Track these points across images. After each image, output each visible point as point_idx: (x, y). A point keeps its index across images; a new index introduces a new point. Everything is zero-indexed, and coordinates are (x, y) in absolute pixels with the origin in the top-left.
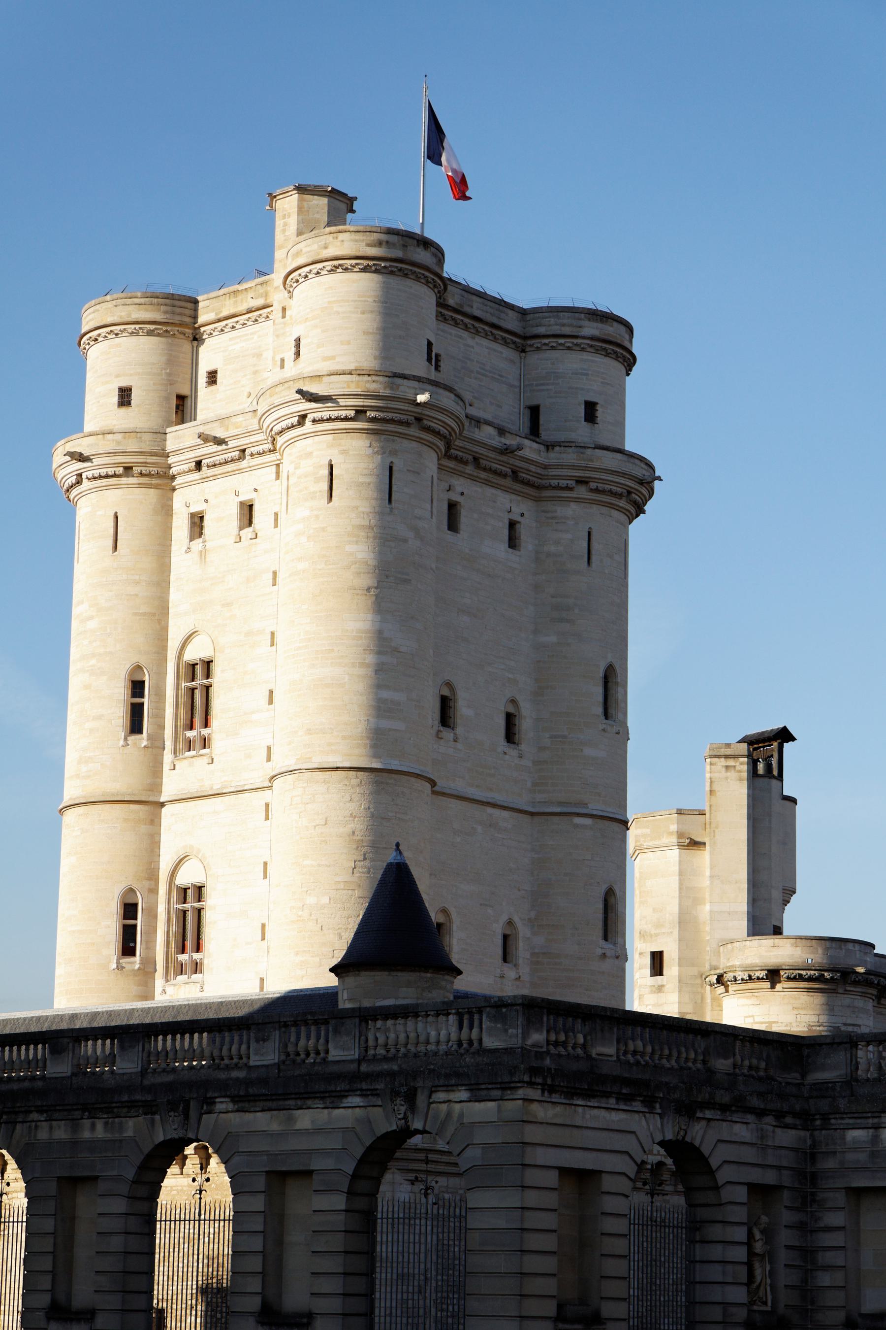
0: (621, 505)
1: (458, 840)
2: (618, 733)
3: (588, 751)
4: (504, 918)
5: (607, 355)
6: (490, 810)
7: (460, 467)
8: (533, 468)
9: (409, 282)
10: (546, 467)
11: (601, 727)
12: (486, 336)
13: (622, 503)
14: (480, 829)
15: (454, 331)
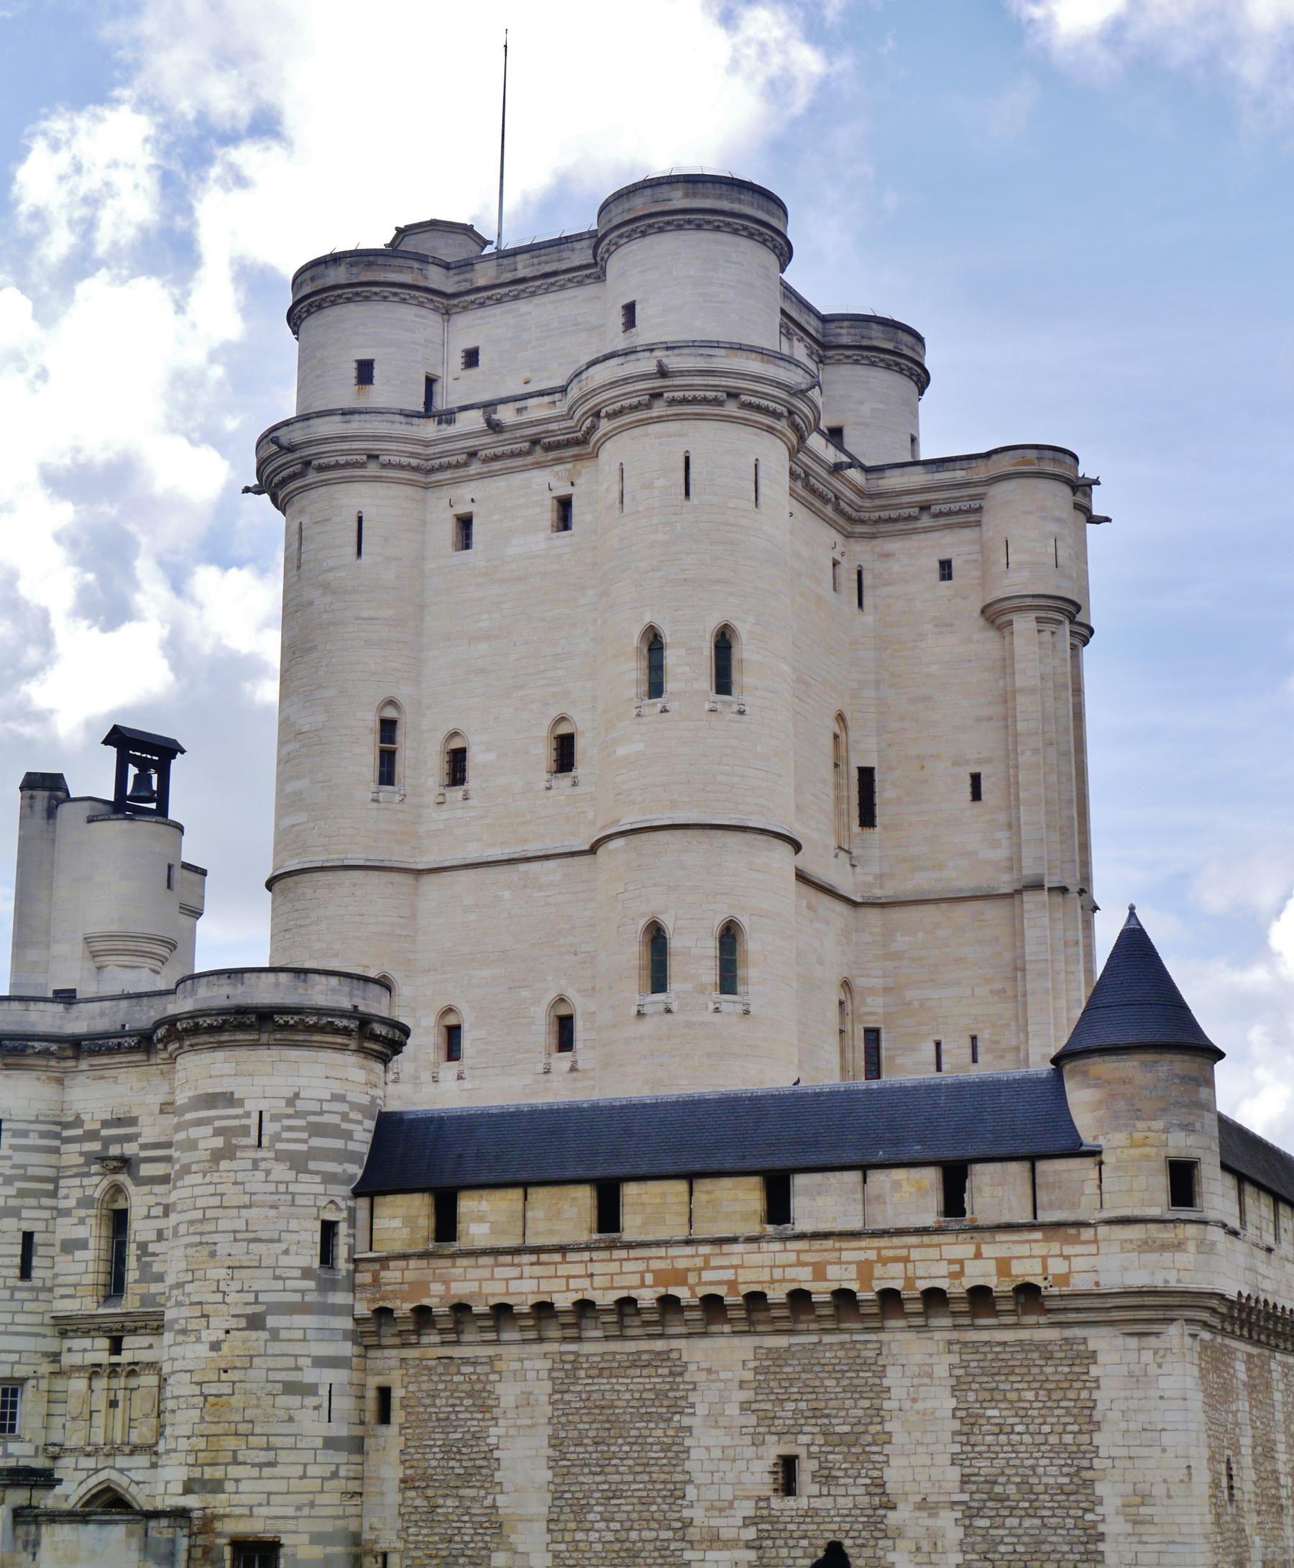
0: (655, 414)
1: (472, 917)
2: (664, 711)
3: (621, 751)
4: (551, 996)
5: (644, 234)
6: (523, 867)
7: (461, 472)
8: (554, 426)
9: (326, 312)
10: (569, 415)
11: (635, 712)
12: (547, 291)
13: (659, 409)
14: (507, 895)
15: (498, 310)
